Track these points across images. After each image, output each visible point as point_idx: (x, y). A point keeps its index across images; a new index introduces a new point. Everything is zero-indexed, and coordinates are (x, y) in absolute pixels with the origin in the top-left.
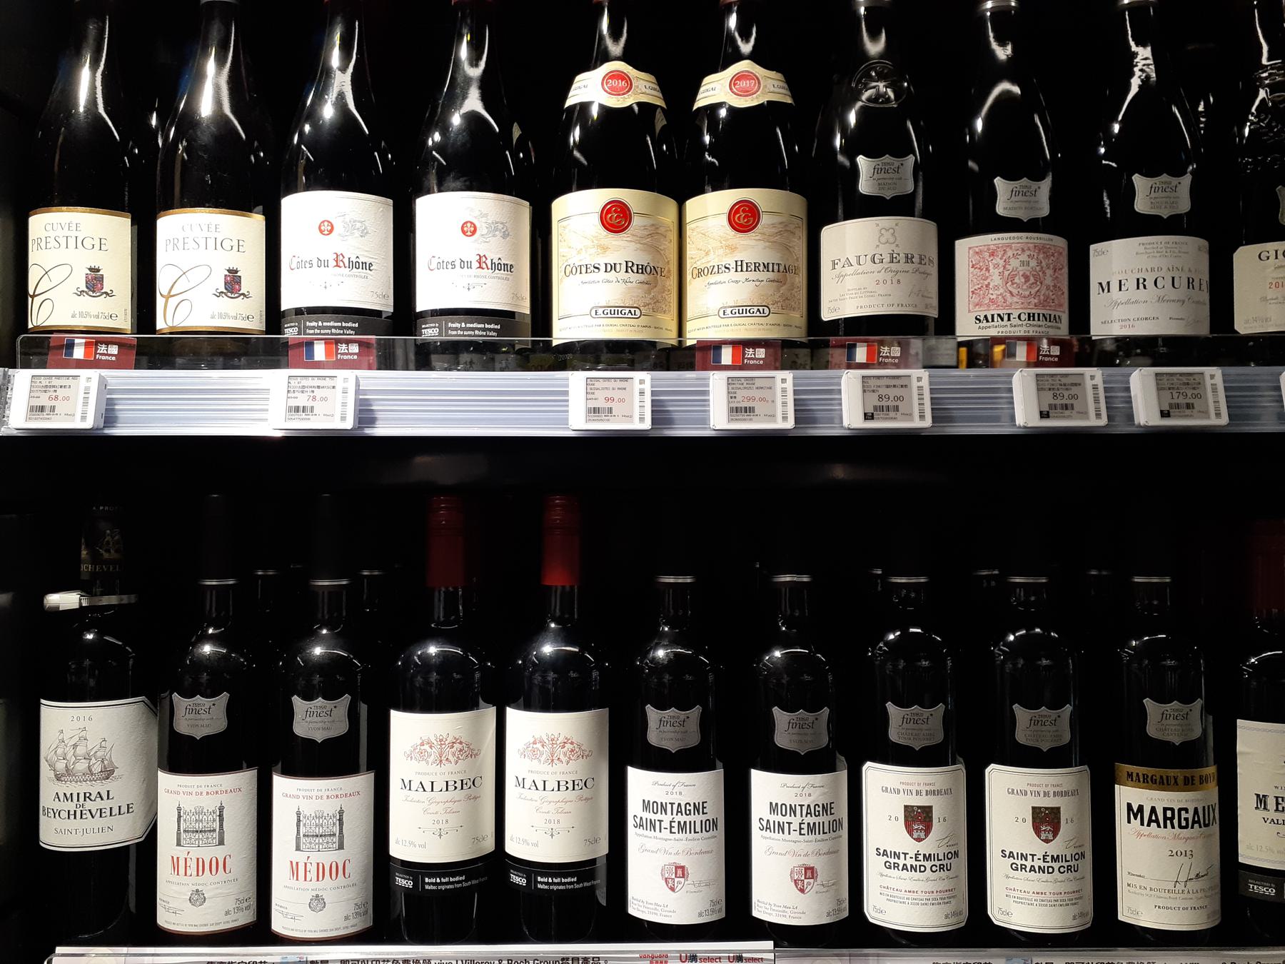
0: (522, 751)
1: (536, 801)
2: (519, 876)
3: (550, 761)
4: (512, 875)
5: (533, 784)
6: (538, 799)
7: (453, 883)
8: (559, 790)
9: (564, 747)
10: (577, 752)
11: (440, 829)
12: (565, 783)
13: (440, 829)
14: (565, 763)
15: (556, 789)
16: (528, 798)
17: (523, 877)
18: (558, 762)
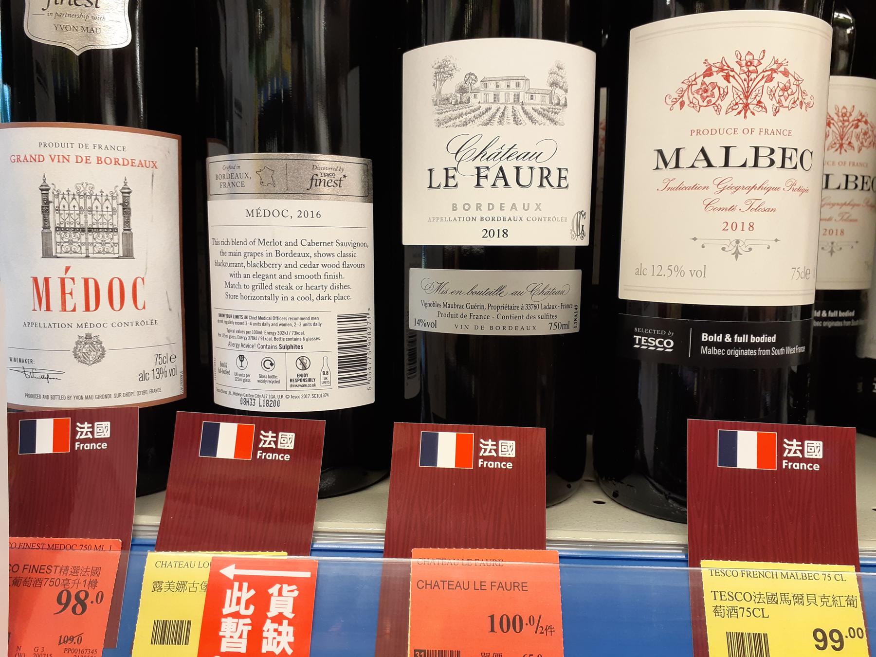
1: (706, 188)
5: (701, 157)
12: (769, 151)
15: (751, 162)
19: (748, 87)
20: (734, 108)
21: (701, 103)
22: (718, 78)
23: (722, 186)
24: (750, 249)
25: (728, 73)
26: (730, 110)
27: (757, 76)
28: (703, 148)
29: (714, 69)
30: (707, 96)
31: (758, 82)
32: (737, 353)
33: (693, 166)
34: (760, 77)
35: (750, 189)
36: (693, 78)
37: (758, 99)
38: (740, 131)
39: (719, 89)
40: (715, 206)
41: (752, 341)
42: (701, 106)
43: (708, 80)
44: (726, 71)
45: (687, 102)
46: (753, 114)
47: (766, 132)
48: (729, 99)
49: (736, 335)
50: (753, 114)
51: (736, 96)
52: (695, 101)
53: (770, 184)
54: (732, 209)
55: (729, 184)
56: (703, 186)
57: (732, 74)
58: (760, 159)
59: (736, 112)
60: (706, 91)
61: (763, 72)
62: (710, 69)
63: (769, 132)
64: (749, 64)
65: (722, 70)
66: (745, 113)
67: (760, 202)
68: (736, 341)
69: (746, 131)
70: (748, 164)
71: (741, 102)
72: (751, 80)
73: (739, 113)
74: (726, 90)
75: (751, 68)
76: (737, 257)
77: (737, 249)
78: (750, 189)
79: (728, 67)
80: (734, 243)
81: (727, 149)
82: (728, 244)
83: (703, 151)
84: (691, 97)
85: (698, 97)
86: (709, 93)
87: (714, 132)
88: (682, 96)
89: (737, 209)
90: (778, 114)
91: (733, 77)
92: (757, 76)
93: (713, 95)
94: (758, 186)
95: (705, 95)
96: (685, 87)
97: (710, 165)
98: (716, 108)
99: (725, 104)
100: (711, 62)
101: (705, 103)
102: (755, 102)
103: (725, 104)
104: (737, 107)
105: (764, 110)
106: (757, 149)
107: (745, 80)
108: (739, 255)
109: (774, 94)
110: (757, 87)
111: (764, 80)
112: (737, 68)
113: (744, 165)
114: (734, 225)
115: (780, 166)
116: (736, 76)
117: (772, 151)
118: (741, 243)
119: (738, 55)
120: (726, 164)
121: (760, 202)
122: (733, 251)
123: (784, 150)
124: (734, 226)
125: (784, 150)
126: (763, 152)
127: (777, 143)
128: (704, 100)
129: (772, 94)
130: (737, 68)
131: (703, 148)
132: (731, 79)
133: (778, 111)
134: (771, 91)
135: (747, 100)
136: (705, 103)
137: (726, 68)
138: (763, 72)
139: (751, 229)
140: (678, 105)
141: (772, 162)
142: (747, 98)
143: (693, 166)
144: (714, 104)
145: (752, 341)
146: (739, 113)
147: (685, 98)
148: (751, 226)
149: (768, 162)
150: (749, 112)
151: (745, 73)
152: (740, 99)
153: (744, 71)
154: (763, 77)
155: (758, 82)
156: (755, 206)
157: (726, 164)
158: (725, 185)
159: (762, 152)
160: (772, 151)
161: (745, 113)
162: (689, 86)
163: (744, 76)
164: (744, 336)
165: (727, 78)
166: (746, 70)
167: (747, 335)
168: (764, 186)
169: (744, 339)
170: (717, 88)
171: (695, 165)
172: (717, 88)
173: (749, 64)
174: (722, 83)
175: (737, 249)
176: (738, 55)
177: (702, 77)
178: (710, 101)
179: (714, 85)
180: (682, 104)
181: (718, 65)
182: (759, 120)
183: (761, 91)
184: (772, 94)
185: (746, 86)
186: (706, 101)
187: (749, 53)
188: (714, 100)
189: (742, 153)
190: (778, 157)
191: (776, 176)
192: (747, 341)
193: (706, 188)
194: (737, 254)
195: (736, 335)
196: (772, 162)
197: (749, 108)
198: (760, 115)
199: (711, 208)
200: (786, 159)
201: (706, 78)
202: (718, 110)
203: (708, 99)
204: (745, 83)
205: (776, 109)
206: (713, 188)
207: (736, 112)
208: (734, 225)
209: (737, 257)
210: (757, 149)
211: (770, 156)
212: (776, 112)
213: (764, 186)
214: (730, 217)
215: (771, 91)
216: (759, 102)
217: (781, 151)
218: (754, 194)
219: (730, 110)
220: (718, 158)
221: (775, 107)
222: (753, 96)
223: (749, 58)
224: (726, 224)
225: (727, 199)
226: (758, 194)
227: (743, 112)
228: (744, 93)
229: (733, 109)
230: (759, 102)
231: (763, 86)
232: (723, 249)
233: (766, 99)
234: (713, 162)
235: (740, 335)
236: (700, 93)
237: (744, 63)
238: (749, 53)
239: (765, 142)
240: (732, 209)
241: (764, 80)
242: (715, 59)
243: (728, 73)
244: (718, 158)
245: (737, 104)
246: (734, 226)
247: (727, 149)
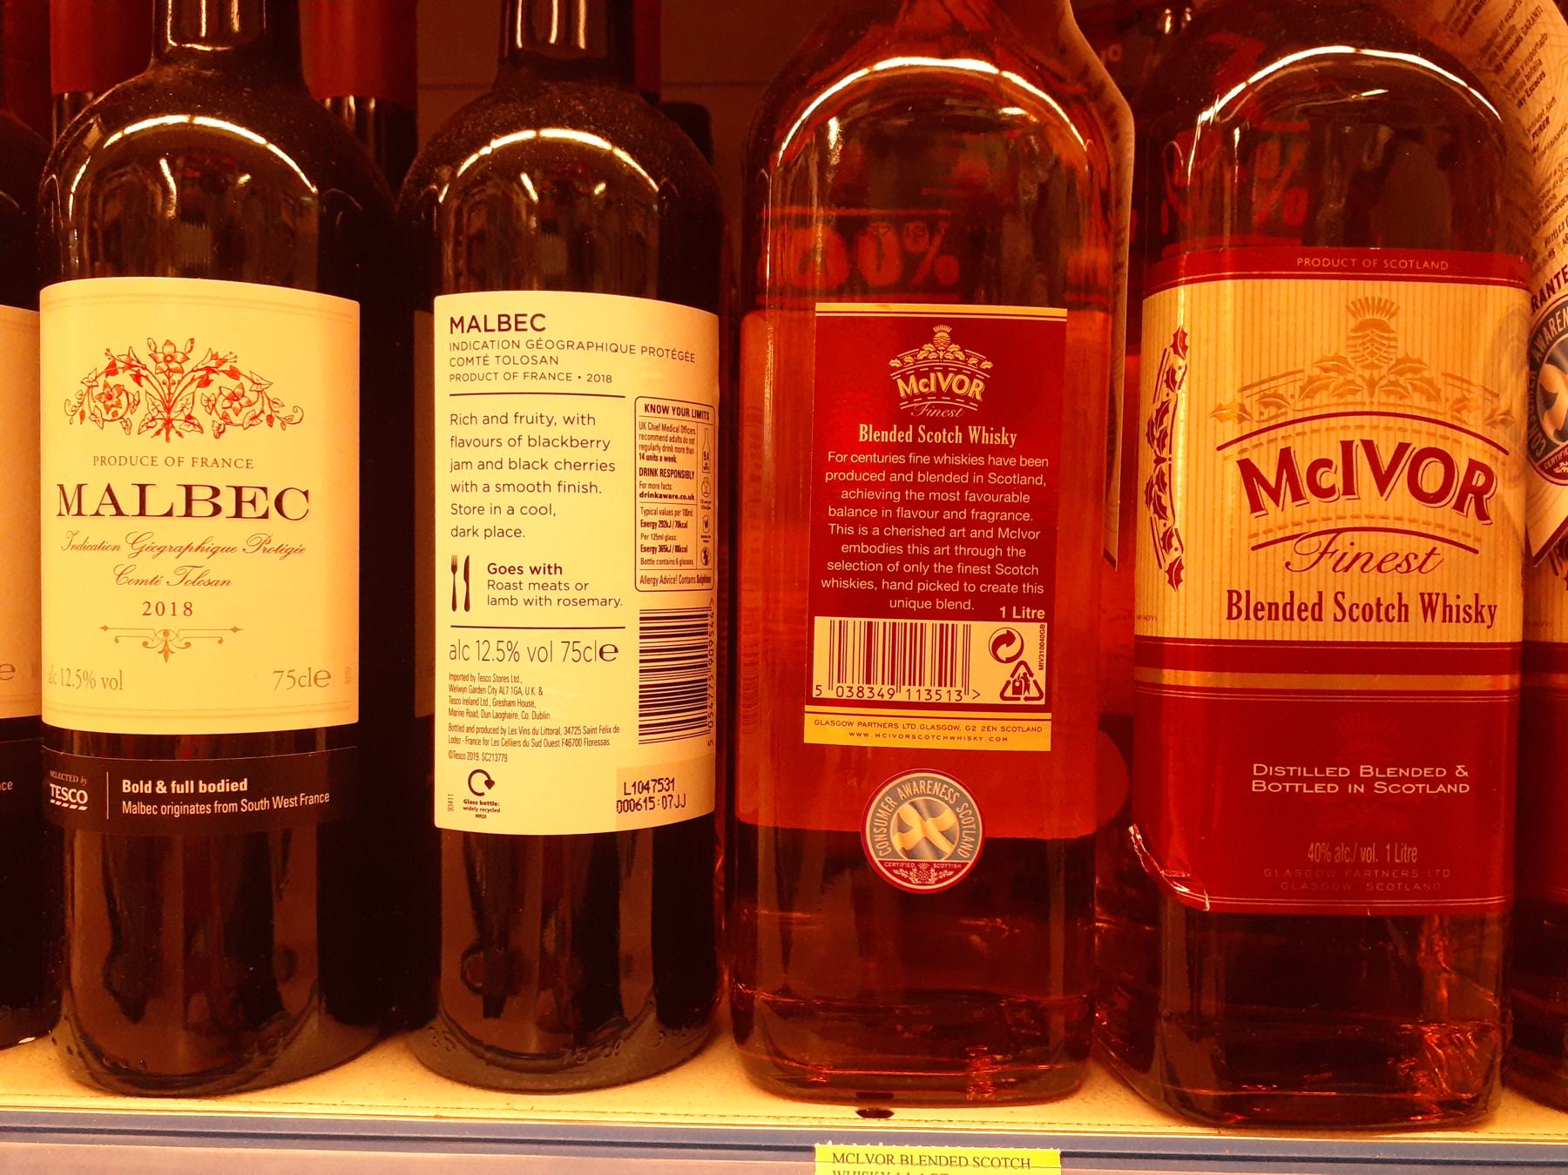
0: (75, 402)
1: (117, 548)
2: (69, 785)
3: (160, 423)
4: (52, 785)
5: (108, 500)
6: (120, 541)
7: (208, 798)
8: (188, 513)
9: (206, 382)
10: (250, 404)
11: (166, 633)
12: (209, 493)
13: (166, 633)
14: (209, 432)
15: (180, 509)
16: (91, 542)
17: (78, 786)
18: (185, 426)
19: (169, 394)
20: (149, 425)
21: (105, 417)
22: (124, 378)
23: (139, 546)
24: (188, 645)
25: (138, 372)
26: (145, 428)
27: (183, 378)
28: (109, 486)
29: (119, 365)
30: (112, 406)
31: (186, 387)
32: (177, 811)
33: (97, 514)
34: (188, 379)
35: (182, 550)
36: (93, 376)
37: (186, 412)
38: (160, 461)
39: (127, 395)
40: (130, 576)
41: (201, 791)
42: (104, 420)
43: (112, 380)
44: (136, 369)
45: (88, 414)
46: (180, 435)
47: (204, 462)
48: (142, 410)
49: (174, 782)
50: (180, 435)
51: (152, 407)
52: (97, 412)
53: (217, 542)
54: (155, 581)
55: (149, 543)
56: (113, 546)
57: (143, 372)
58: (195, 505)
59: (152, 432)
60: (110, 398)
61: (193, 371)
62: (113, 365)
63: (209, 463)
64: (169, 359)
65: (129, 366)
66: (168, 433)
67: (202, 570)
68: (173, 791)
69: (170, 461)
70: (176, 513)
71: (160, 416)
72: (174, 383)
73: (158, 433)
74: (137, 398)
75: (173, 365)
76: (166, 657)
77: (166, 644)
78: (182, 550)
79: (138, 362)
80: (161, 635)
81: (142, 488)
82: (152, 636)
83: (109, 490)
84: (93, 405)
85: (101, 406)
86: (114, 401)
87: (123, 461)
88: (81, 403)
89: (164, 581)
90: (223, 435)
91: (146, 377)
92: (183, 378)
93: (119, 405)
94: (195, 546)
95: (109, 403)
96: (84, 389)
97: (119, 513)
98: (124, 424)
99: (137, 418)
100: (114, 353)
101: (109, 417)
102: (182, 417)
103: (137, 418)
104: (154, 423)
105: (198, 429)
106: (189, 489)
107: (164, 384)
108: (170, 655)
109: (214, 406)
110: (184, 394)
111: (195, 384)
112: (151, 365)
113: (169, 514)
114: (160, 606)
115: (233, 514)
116: (150, 377)
117: (216, 492)
118: (172, 636)
119: (151, 344)
120: (142, 513)
121: (202, 570)
122: (161, 648)
123: (239, 490)
124: (160, 609)
125: (239, 490)
126: (200, 493)
127: (225, 479)
128: (108, 409)
129: (211, 406)
130: (151, 365)
131: (109, 486)
132: (143, 381)
133: (223, 432)
134: (209, 400)
135: (169, 413)
136: (109, 417)
137: (134, 363)
138: (193, 371)
139: (188, 612)
140: (77, 417)
141: (217, 510)
142: (168, 410)
143: (97, 514)
144: (121, 418)
145: (201, 791)
146: (158, 433)
147: (85, 407)
148: (188, 608)
149: (210, 509)
150: (172, 432)
151: (164, 372)
152: (159, 412)
153: (161, 369)
154: (193, 380)
155: (186, 387)
156: (192, 577)
157: (142, 513)
158: (142, 544)
159: (197, 493)
160: (216, 492)
161: (168, 433)
162: (89, 387)
163: (162, 377)
164: (187, 782)
165: (137, 378)
166: (165, 368)
167: (192, 782)
168: (206, 546)
169: (187, 787)
170: (124, 394)
171: (101, 512)
172: (124, 394)
173: (169, 358)
174: (131, 386)
175: (166, 644)
176: (151, 344)
177: (104, 375)
178: (115, 414)
179: (120, 389)
180: (82, 415)
181: (123, 358)
182: (190, 444)
183: (190, 401)
184: (211, 404)
185: (166, 392)
186: (110, 413)
187: (168, 343)
188: (121, 412)
189: (165, 495)
190: (227, 501)
191: (225, 530)
192: (192, 791)
193: (117, 548)
194: (166, 652)
195: (174, 782)
196: (217, 510)
197: (173, 427)
198: (191, 436)
199: (125, 580)
200: (244, 504)
201: (110, 377)
202: (127, 427)
203: (113, 409)
204: (165, 388)
205: (219, 428)
206: (126, 549)
207: (152, 432)
208: (160, 606)
209: (166, 657)
210: (189, 489)
211: (212, 500)
212: (219, 433)
213: (206, 546)
214: (155, 594)
215: (209, 400)
216: (189, 417)
217: (233, 492)
218: (189, 558)
219: (145, 428)
220: (130, 503)
221: (216, 425)
222: (178, 407)
223: (169, 349)
224: (147, 605)
225: (147, 566)
226: (199, 558)
227: (164, 431)
228: (163, 403)
229: (148, 427)
230: (189, 417)
231: (194, 393)
232: (145, 644)
233: (199, 413)
234: (124, 510)
235: (181, 782)
236: (103, 400)
237: (160, 357)
238: (168, 343)
239: (201, 477)
240: (155, 581)
241: (195, 384)
242: (119, 350)
243: (138, 372)
244: (130, 503)
245: (153, 419)
246: (160, 609)
247: (142, 488)
